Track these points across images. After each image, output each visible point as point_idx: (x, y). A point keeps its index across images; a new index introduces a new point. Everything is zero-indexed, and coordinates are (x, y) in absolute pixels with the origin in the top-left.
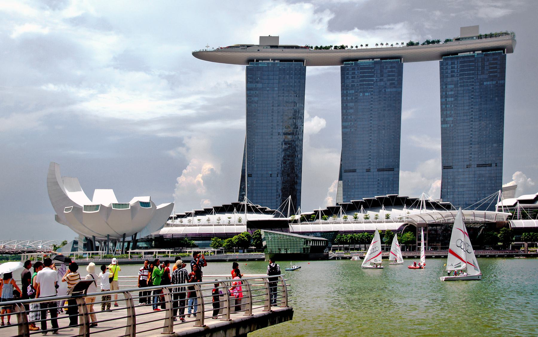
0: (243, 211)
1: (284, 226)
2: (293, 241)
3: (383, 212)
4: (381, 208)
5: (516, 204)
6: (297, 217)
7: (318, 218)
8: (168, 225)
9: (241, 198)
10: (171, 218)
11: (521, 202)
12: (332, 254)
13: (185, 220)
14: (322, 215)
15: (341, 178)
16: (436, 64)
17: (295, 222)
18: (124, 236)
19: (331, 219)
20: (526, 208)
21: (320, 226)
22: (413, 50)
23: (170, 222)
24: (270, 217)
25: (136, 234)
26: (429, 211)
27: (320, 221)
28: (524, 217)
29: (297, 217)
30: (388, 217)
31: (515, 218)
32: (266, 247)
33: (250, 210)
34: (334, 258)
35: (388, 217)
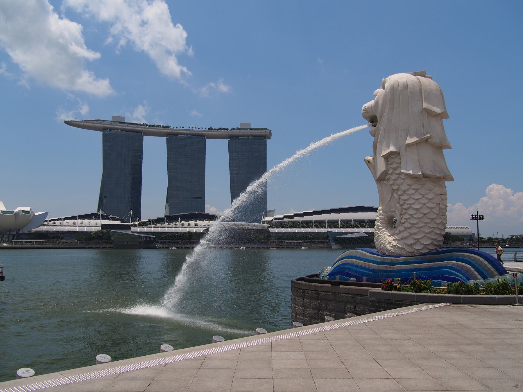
1: (128, 227)
2: (132, 237)
6: (137, 223)
8: (44, 225)
9: (98, 211)
10: (46, 221)
11: (275, 219)
12: (158, 245)
13: (57, 223)
14: (153, 222)
16: (226, 141)
18: (10, 231)
19: (159, 225)
20: (277, 222)
21: (152, 229)
22: (211, 132)
23: (46, 223)
24: (118, 223)
25: (19, 230)
29: (137, 223)
30: (196, 225)
32: (113, 240)
33: (104, 218)
34: (160, 248)
35: (196, 225)
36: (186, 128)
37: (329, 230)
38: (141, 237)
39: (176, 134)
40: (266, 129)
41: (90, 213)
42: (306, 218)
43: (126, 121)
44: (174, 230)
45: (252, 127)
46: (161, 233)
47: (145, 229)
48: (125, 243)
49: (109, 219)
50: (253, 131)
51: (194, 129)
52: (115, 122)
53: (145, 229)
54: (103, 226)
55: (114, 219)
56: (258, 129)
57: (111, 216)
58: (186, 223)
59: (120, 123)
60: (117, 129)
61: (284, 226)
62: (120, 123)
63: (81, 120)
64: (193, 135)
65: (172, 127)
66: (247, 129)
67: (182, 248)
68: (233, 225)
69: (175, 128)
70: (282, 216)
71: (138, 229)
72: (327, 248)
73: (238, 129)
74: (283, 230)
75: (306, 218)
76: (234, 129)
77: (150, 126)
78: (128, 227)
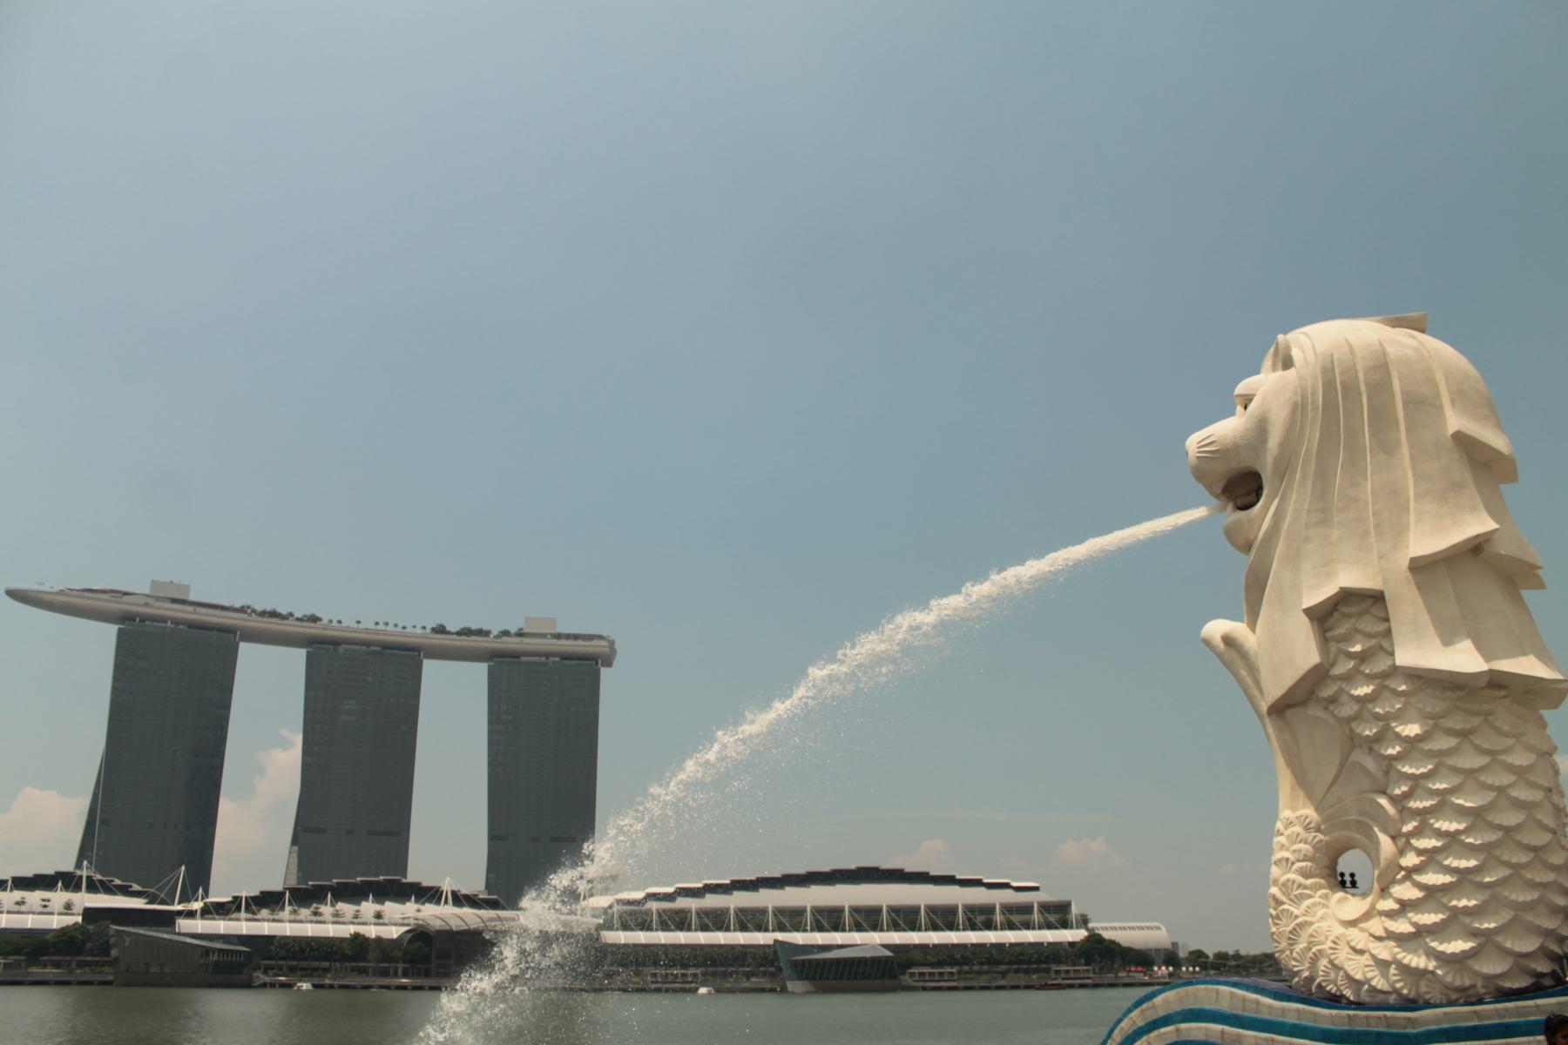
0: (77, 888)
1: (168, 919)
3: (368, 907)
4: (366, 899)
5: (611, 907)
6: (197, 906)
7: (238, 909)
9: (79, 865)
11: (619, 901)
12: (261, 977)
15: (295, 841)
17: (191, 914)
19: (265, 913)
20: (631, 913)
21: (242, 926)
22: (440, 640)
24: (138, 903)
26: (457, 910)
27: (243, 914)
28: (625, 927)
30: (379, 916)
31: (608, 926)
32: (117, 959)
33: (93, 887)
34: (264, 985)
35: (379, 916)
36: (368, 624)
37: (780, 936)
38: (207, 952)
39: (336, 643)
40: (601, 637)
41: (51, 872)
42: (712, 901)
43: (192, 598)
44: (310, 930)
45: (561, 629)
46: (270, 939)
47: (221, 926)
48: (154, 969)
49: (108, 889)
50: (563, 642)
51: (390, 628)
52: (157, 599)
53: (221, 926)
54: (90, 914)
55: (125, 891)
56: (576, 637)
57: (118, 882)
58: (346, 908)
59: (174, 601)
60: (163, 620)
61: (645, 926)
62: (174, 601)
63: (56, 589)
64: (387, 647)
65: (325, 621)
66: (544, 636)
67: (331, 986)
68: (491, 920)
69: (335, 623)
70: (639, 895)
71: (200, 926)
72: (773, 990)
73: (520, 634)
74: (642, 937)
75: (712, 901)
76: (506, 633)
77: (263, 614)
78: (168, 919)
